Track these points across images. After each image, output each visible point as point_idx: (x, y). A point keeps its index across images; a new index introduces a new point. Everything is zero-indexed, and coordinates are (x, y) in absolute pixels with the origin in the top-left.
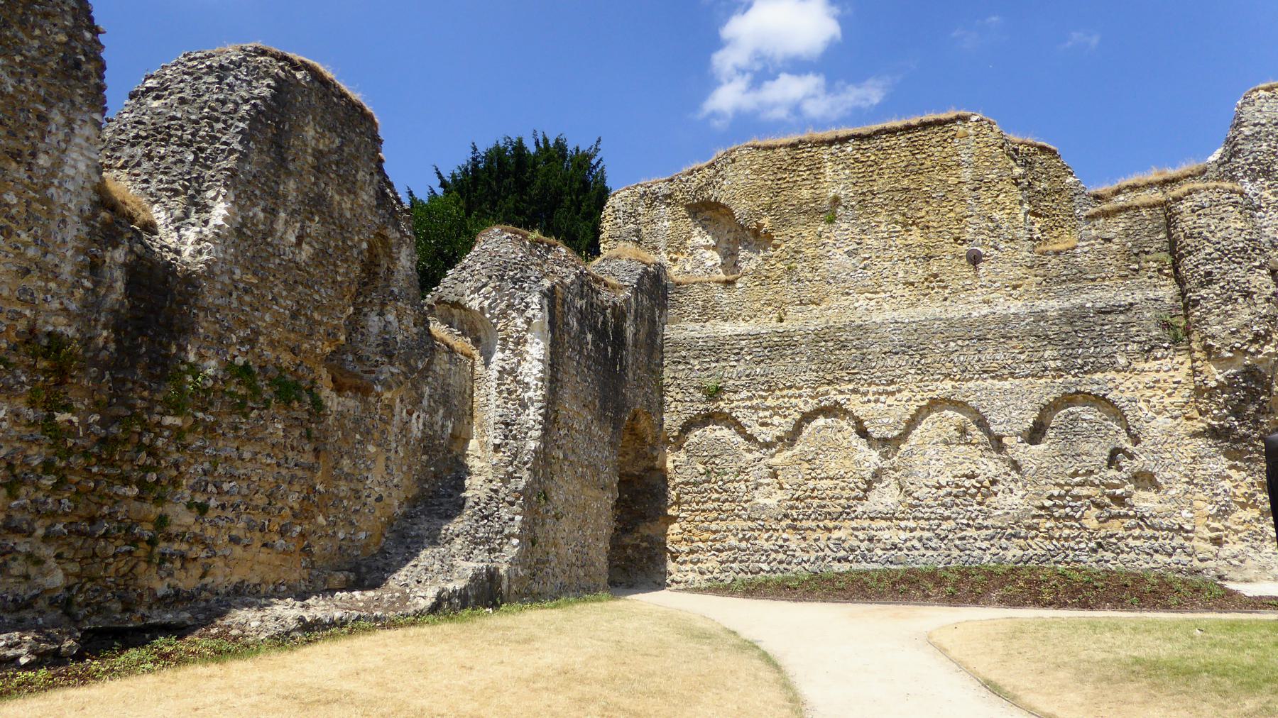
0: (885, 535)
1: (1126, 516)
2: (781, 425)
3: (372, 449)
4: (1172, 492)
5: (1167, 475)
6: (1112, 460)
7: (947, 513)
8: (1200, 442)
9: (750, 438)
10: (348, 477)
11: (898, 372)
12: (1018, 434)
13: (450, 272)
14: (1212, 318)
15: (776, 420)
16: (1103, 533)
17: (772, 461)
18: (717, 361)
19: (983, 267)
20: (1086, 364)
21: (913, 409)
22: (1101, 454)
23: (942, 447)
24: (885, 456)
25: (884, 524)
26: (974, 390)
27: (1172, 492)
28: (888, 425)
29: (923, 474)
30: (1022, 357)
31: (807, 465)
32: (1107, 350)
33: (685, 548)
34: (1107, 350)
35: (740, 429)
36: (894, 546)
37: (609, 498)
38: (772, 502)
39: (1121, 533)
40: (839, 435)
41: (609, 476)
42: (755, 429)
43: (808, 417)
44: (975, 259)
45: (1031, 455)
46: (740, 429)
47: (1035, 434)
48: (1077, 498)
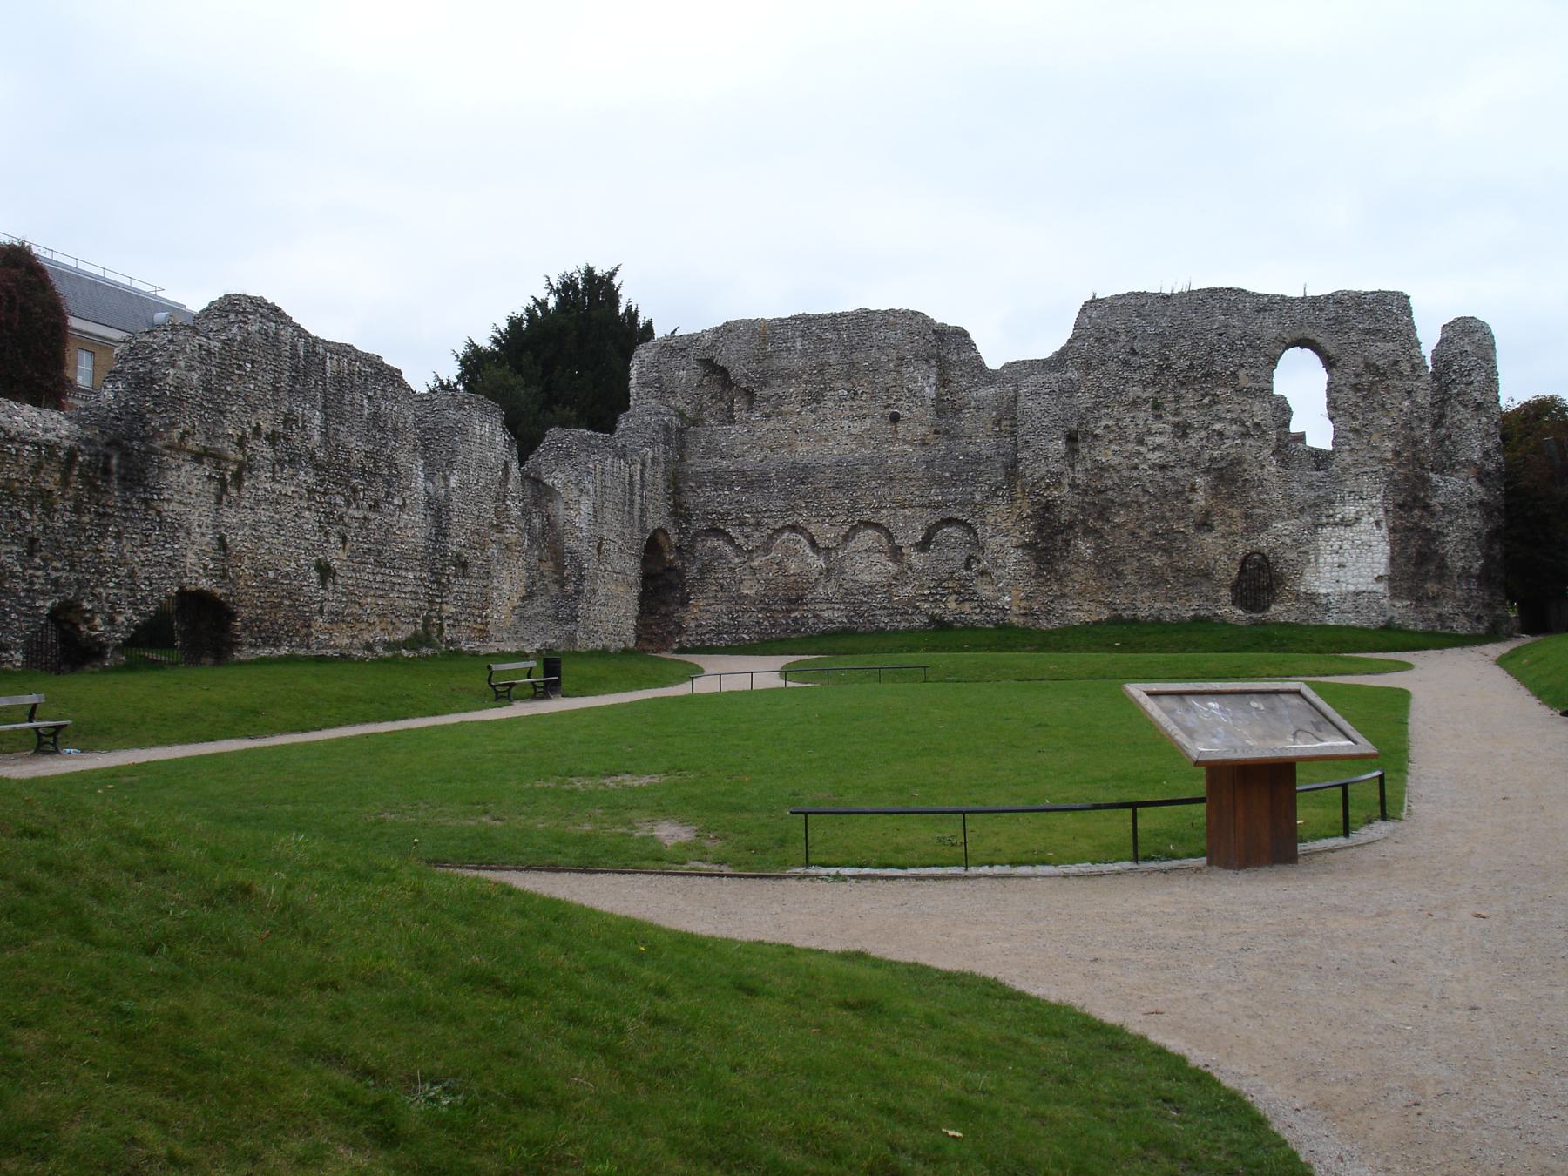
0: (825, 614)
1: (972, 600)
2: (757, 539)
3: (505, 573)
4: (1000, 585)
5: (998, 573)
6: (968, 567)
7: (865, 599)
8: (1020, 552)
9: (739, 547)
10: (497, 588)
11: (838, 502)
12: (911, 546)
13: (531, 457)
14: (1028, 473)
15: (756, 535)
16: (958, 611)
17: (755, 564)
18: (715, 490)
19: (900, 427)
20: (956, 499)
21: (847, 528)
22: (960, 559)
23: (864, 555)
24: (827, 560)
25: (825, 606)
26: (885, 517)
27: (1000, 585)
28: (829, 539)
29: (851, 572)
30: (918, 493)
31: (775, 567)
32: (969, 490)
33: (692, 624)
34: (969, 490)
35: (730, 540)
36: (831, 621)
37: (636, 592)
38: (752, 593)
39: (969, 610)
40: (798, 546)
41: (633, 577)
42: (741, 541)
43: (778, 531)
44: (895, 418)
45: (915, 558)
46: (730, 540)
47: (923, 546)
48: (944, 588)
